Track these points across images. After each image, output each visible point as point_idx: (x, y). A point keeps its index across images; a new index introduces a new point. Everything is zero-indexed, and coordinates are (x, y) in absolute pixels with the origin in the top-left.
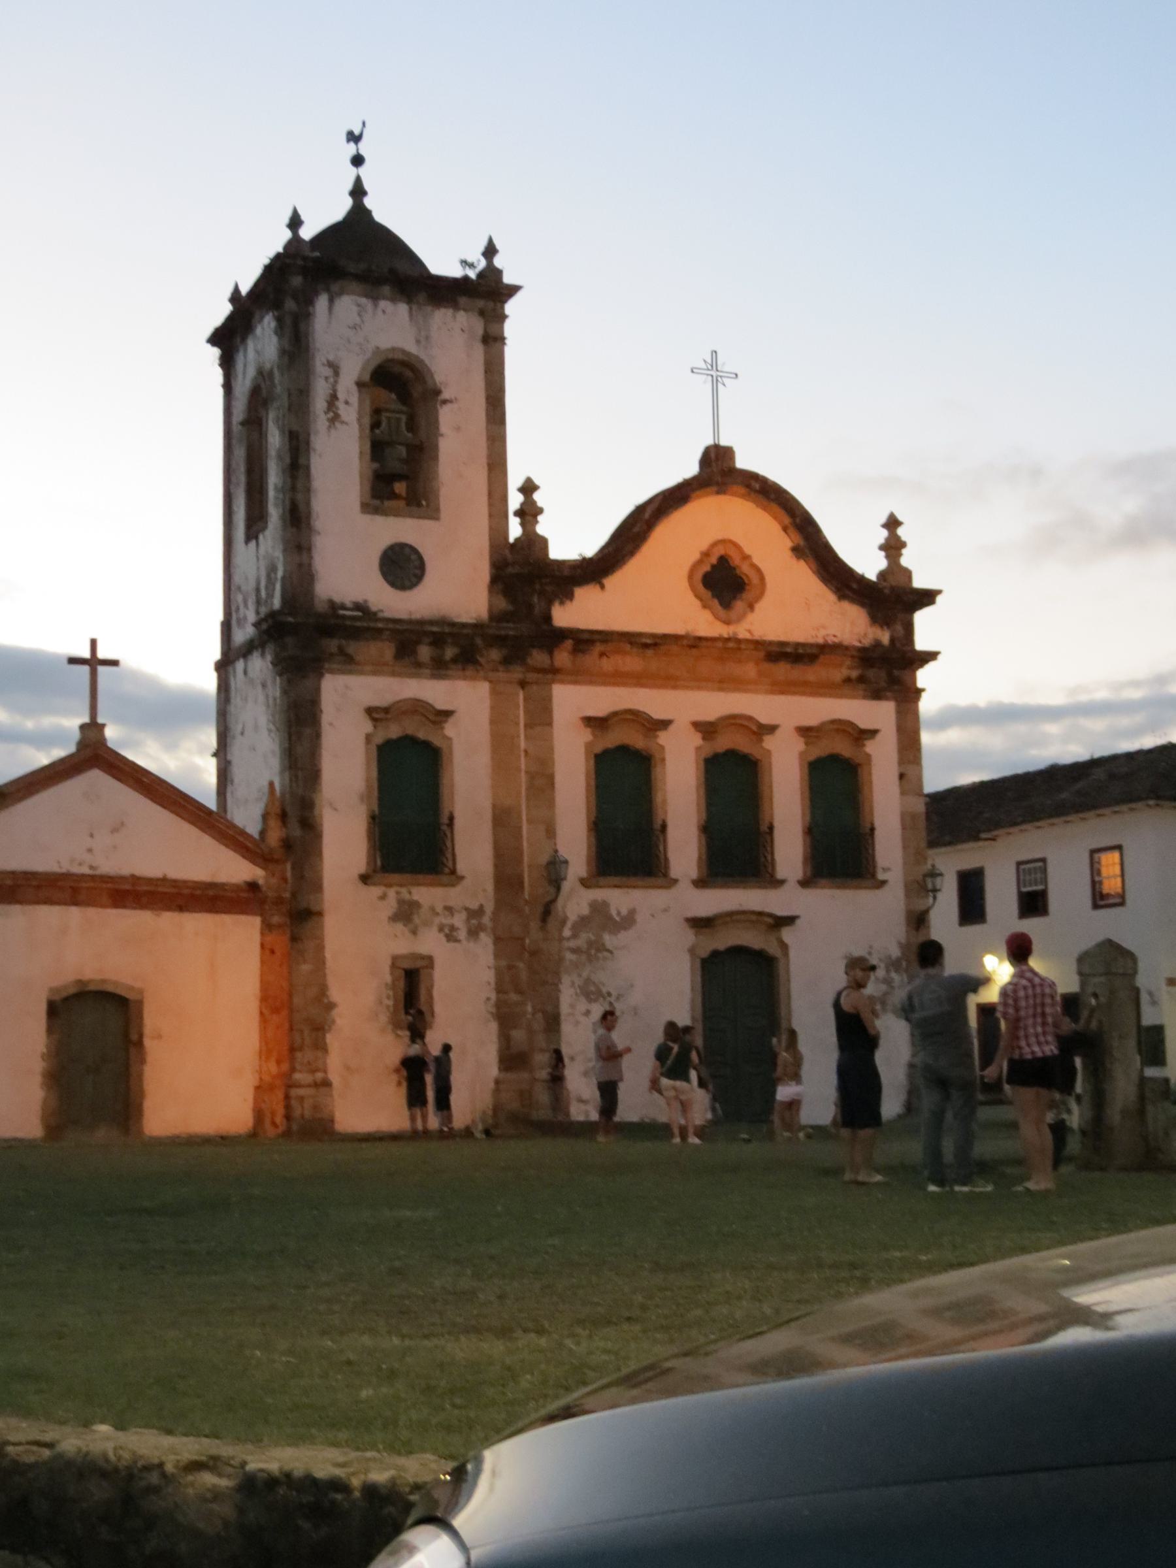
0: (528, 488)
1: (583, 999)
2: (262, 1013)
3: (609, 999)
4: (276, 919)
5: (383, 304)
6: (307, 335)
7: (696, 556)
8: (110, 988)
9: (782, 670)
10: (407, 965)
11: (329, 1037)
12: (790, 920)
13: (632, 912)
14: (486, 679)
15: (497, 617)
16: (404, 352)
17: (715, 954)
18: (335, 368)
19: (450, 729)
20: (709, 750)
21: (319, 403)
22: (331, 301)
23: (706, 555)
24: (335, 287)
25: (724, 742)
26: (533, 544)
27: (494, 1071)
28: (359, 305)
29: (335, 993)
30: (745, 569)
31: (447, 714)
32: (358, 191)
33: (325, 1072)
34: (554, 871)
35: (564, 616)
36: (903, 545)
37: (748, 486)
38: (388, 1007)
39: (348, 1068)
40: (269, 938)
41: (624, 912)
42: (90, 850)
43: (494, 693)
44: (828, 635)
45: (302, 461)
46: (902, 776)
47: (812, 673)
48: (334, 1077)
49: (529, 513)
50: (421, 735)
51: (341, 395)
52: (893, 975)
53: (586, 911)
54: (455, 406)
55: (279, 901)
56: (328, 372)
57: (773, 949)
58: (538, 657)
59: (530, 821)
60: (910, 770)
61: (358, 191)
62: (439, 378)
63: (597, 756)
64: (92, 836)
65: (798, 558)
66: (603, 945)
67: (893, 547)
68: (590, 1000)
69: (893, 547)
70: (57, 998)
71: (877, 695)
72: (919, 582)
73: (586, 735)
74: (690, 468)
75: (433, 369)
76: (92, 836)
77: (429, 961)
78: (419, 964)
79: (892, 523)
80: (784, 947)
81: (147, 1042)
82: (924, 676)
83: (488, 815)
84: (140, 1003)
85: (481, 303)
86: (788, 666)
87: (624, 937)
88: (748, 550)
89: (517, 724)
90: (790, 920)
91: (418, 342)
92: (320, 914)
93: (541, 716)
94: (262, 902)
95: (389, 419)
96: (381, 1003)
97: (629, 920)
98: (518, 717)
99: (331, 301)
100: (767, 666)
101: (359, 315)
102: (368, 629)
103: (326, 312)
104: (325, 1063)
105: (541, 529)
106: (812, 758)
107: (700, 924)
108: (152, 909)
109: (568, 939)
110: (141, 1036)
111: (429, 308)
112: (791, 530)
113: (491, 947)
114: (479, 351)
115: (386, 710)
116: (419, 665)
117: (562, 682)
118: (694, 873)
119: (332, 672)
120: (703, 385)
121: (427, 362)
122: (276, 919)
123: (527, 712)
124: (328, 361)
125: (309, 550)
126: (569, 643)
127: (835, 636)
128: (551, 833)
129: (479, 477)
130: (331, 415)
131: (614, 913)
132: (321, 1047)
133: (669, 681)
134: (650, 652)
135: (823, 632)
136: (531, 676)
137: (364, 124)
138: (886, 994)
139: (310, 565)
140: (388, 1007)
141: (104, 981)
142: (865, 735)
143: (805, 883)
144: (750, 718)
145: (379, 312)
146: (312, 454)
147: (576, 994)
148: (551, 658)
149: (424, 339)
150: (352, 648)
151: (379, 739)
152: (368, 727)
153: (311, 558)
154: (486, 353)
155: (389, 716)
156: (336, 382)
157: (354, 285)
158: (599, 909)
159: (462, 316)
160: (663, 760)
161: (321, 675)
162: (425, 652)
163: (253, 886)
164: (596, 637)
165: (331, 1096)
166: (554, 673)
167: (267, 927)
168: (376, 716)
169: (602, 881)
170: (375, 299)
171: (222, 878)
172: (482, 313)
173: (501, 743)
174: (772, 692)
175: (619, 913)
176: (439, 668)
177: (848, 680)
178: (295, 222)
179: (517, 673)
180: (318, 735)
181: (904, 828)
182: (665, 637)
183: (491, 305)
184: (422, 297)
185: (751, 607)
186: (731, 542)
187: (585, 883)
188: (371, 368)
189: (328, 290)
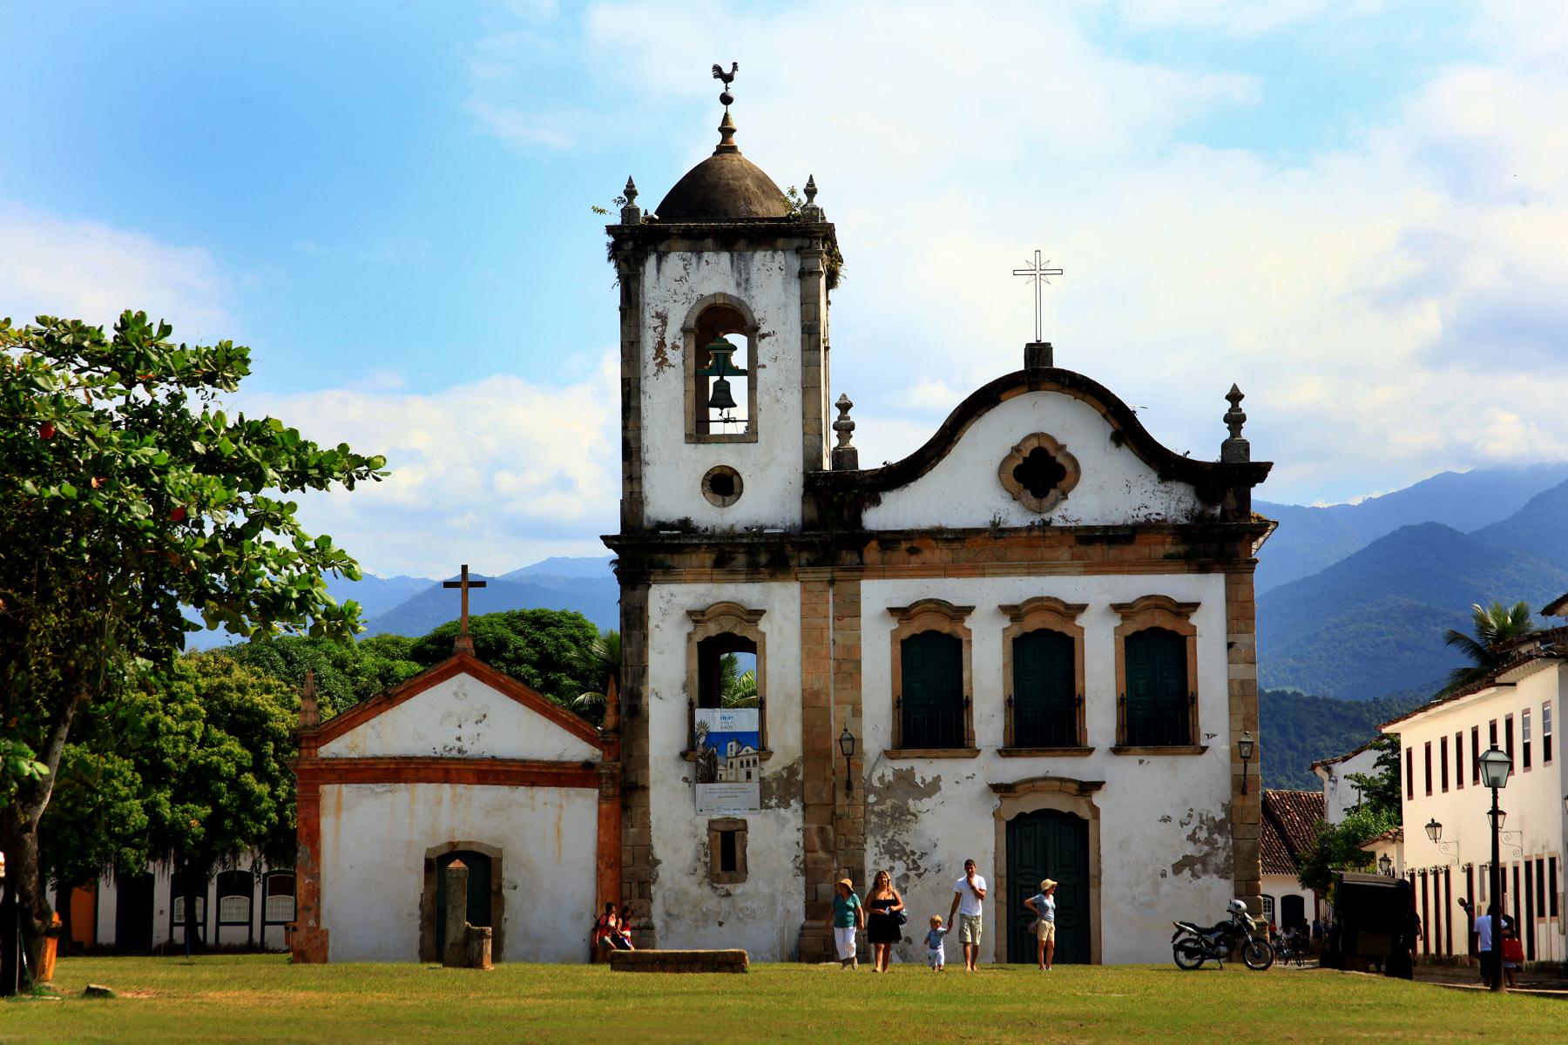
0: (845, 407)
1: (887, 857)
2: (598, 869)
3: (912, 857)
4: (611, 791)
5: (707, 255)
6: (637, 295)
7: (1006, 451)
8: (475, 848)
9: (1097, 551)
10: (722, 827)
11: (653, 888)
12: (1098, 785)
13: (937, 779)
14: (797, 579)
15: (807, 525)
16: (724, 295)
17: (1021, 816)
18: (663, 318)
19: (763, 625)
20: (1017, 630)
21: (649, 351)
22: (659, 260)
23: (1017, 449)
24: (662, 247)
25: (1033, 623)
26: (846, 457)
27: (801, 919)
28: (684, 260)
29: (659, 851)
30: (1060, 459)
31: (760, 613)
32: (726, 130)
33: (650, 918)
34: (852, 744)
35: (876, 518)
36: (1226, 419)
37: (1057, 382)
38: (706, 863)
39: (669, 914)
40: (604, 807)
41: (929, 780)
42: (459, 739)
43: (804, 591)
44: (1150, 514)
45: (633, 404)
46: (1230, 645)
47: (1129, 553)
48: (657, 922)
49: (845, 429)
50: (737, 632)
51: (668, 342)
52: (1216, 836)
53: (889, 777)
54: (773, 338)
55: (613, 776)
56: (657, 322)
57: (1083, 812)
58: (849, 558)
59: (836, 703)
60: (1242, 639)
61: (726, 130)
62: (757, 315)
63: (903, 643)
64: (460, 726)
65: (1118, 445)
66: (908, 809)
67: (1235, 420)
68: (893, 858)
69: (1235, 420)
70: (433, 856)
71: (1204, 569)
72: (1255, 457)
73: (893, 624)
74: (1018, 364)
75: (753, 307)
76: (460, 726)
77: (743, 826)
78: (734, 827)
79: (1235, 397)
80: (1096, 811)
81: (505, 891)
82: (1261, 549)
83: (798, 699)
84: (500, 860)
85: (797, 242)
86: (1105, 547)
87: (926, 803)
88: (1061, 441)
89: (826, 617)
90: (1098, 785)
91: (738, 285)
92: (645, 788)
93: (850, 609)
94: (599, 776)
95: (716, 355)
96: (699, 859)
97: (933, 787)
98: (827, 610)
99: (659, 260)
100: (1081, 549)
101: (685, 268)
102: (687, 545)
103: (655, 272)
104: (649, 910)
105: (853, 443)
106: (1129, 632)
107: (1003, 790)
108: (509, 785)
109: (874, 804)
110: (500, 887)
111: (750, 253)
112: (1110, 417)
113: (800, 812)
114: (795, 288)
115: (702, 613)
116: (733, 572)
117: (868, 578)
118: (1000, 745)
119: (655, 582)
120: (1026, 286)
121: (748, 303)
122: (611, 791)
123: (835, 607)
124: (657, 313)
125: (640, 479)
126: (874, 544)
127: (1158, 514)
128: (857, 712)
129: (794, 399)
130: (660, 359)
131: (918, 780)
132: (646, 896)
133: (974, 569)
134: (956, 545)
135: (1144, 511)
136: (838, 574)
137: (735, 64)
138: (1208, 854)
139: (640, 493)
140: (706, 863)
141: (470, 843)
142: (1186, 609)
143: (1117, 750)
144: (1056, 600)
145: (703, 263)
146: (642, 396)
147: (881, 853)
148: (861, 556)
149: (744, 282)
150: (676, 560)
151: (699, 638)
152: (689, 627)
153: (641, 486)
154: (801, 287)
155: (705, 618)
156: (664, 331)
157: (681, 243)
158: (905, 778)
159: (780, 256)
160: (970, 642)
161: (650, 586)
162: (741, 559)
163: (588, 765)
164: (897, 536)
165: (653, 936)
166: (862, 570)
167: (602, 798)
168: (694, 618)
169: (905, 752)
170: (699, 252)
171: (567, 757)
172: (798, 251)
173: (810, 636)
174: (1086, 573)
175: (923, 780)
176: (754, 573)
177: (1169, 557)
178: (631, 192)
179: (826, 574)
180: (646, 637)
181: (1231, 696)
182: (964, 531)
183: (807, 242)
184: (742, 244)
185: (1065, 496)
186: (1043, 434)
187: (889, 755)
188: (696, 312)
189: (656, 250)
